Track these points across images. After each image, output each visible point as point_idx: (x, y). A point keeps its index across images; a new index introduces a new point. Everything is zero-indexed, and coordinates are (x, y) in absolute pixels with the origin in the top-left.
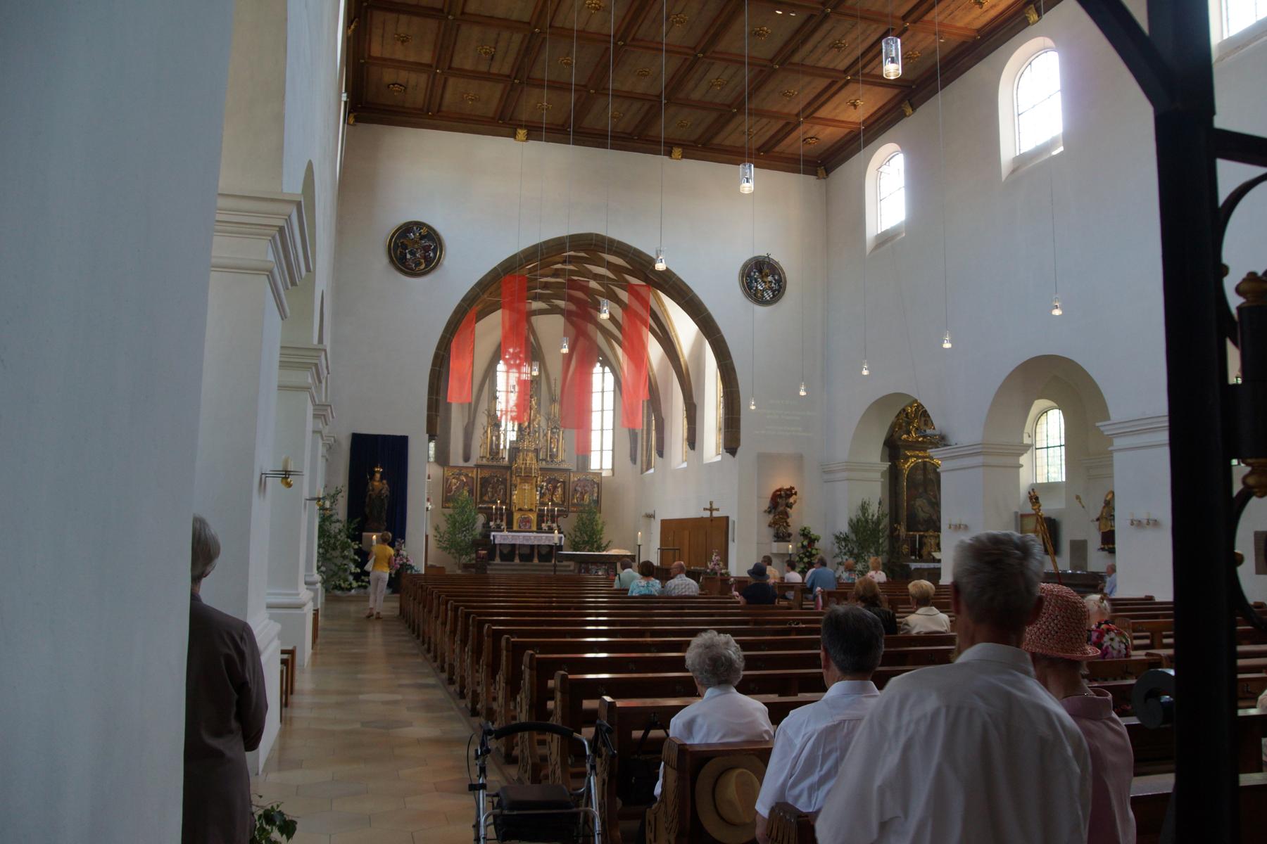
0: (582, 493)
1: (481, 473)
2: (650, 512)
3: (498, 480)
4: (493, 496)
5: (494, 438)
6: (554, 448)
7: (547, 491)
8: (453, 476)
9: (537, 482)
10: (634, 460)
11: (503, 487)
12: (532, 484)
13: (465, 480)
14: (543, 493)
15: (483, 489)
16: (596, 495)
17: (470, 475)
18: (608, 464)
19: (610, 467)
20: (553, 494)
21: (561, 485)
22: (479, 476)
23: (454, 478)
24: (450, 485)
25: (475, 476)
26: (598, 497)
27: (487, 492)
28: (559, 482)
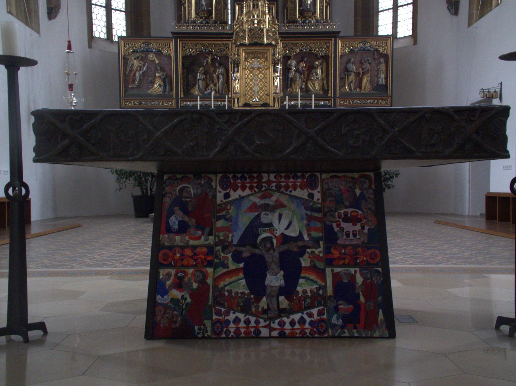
0: (357, 74)
1: (183, 47)
3: (213, 60)
4: (207, 86)
7: (298, 75)
8: (138, 55)
9: (274, 55)
11: (221, 70)
12: (266, 59)
13: (157, 62)
14: (292, 78)
15: (190, 76)
16: (382, 76)
19: (410, 33)
20: (308, 79)
21: (321, 64)
22: (180, 55)
23: (138, 58)
24: (131, 71)
25: (173, 54)
26: (386, 78)
28: (317, 59)
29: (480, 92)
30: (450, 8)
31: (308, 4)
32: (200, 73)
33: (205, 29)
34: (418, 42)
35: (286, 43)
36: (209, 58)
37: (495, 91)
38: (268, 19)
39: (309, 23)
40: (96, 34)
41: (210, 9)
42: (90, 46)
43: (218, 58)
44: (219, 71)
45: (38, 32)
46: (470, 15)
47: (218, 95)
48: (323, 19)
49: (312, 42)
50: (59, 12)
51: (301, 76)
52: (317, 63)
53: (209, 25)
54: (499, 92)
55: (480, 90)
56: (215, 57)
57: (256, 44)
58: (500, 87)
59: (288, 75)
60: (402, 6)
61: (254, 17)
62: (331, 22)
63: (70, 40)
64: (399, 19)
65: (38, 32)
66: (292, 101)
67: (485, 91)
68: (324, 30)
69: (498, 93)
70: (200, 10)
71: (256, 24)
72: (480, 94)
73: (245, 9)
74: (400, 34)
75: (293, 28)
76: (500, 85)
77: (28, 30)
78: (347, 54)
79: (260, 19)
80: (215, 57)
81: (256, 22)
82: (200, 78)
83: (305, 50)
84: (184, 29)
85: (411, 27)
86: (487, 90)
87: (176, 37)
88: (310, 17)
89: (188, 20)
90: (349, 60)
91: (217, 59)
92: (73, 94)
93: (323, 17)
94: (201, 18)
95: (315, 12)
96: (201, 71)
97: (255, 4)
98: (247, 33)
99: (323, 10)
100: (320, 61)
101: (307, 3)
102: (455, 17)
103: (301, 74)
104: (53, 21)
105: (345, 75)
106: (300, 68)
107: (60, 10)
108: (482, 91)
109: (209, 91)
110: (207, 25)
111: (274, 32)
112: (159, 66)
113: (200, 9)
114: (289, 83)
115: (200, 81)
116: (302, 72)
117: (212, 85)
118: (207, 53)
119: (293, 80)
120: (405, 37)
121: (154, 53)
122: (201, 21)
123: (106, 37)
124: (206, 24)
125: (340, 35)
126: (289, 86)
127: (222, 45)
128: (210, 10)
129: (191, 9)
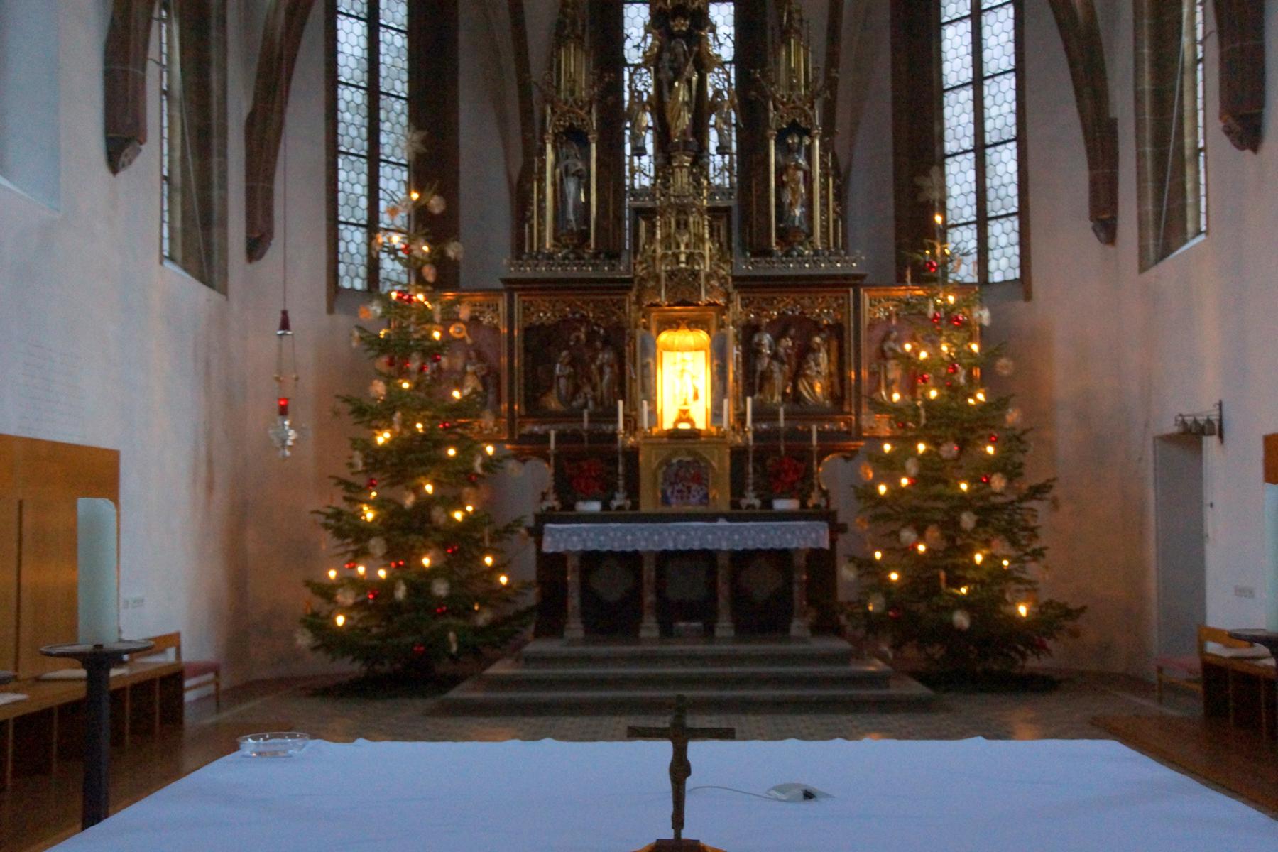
2: (1204, 408)
3: (592, 335)
4: (577, 389)
5: (571, 186)
6: (791, 204)
7: (776, 366)
10: (1106, 228)
11: (605, 356)
13: (469, 341)
14: (763, 373)
15: (540, 369)
17: (486, 320)
18: (1004, 266)
19: (1015, 274)
20: (797, 375)
21: (825, 340)
27: (551, 382)
29: (1176, 420)
30: (1097, 229)
31: (795, 216)
32: (561, 362)
33: (574, 271)
34: (1034, 295)
35: (748, 298)
36: (580, 330)
37: (1209, 421)
38: (710, 250)
39: (799, 255)
40: (345, 283)
41: (584, 228)
42: (331, 310)
43: (602, 331)
44: (603, 358)
45: (223, 290)
46: (1142, 249)
47: (600, 410)
48: (828, 248)
49: (807, 295)
50: (270, 244)
51: (783, 369)
52: (818, 340)
53: (582, 262)
54: (1216, 424)
55: (1176, 418)
56: (596, 328)
57: (683, 303)
58: (1217, 412)
59: (755, 366)
60: (997, 218)
61: (678, 247)
62: (846, 255)
63: (288, 308)
64: (991, 242)
65: (223, 290)
66: (764, 421)
67: (1187, 418)
68: (832, 272)
69: (1213, 424)
70: (564, 231)
71: (683, 262)
72: (1176, 425)
73: (658, 232)
74: (996, 277)
75: (762, 268)
76: (1218, 407)
77: (204, 289)
78: (883, 322)
79: (692, 251)
80: (596, 328)
81: (683, 258)
82: (561, 374)
83: (790, 313)
84: (528, 272)
85: (1016, 261)
86: (1192, 418)
87: (510, 288)
88: (801, 243)
89: (539, 252)
90: (891, 332)
91: (598, 332)
92: (287, 423)
93: (828, 244)
94: (566, 246)
95: (811, 233)
96: (565, 358)
97: (682, 222)
98: (663, 282)
99: (828, 228)
100: (824, 335)
101: (792, 214)
102: (1109, 249)
103: (782, 362)
104: (256, 264)
105: (879, 367)
106: (781, 350)
107: (273, 242)
108: (1180, 418)
109: (581, 401)
110: (577, 262)
111: (724, 277)
112: (475, 351)
113: (562, 228)
114: (757, 381)
115: (562, 382)
116: (785, 359)
117: (587, 389)
118: (578, 320)
119: (766, 377)
120: (1005, 282)
121: (465, 323)
122: (565, 254)
123: (366, 287)
124: (575, 259)
125: (865, 282)
126: (757, 389)
127: (610, 303)
128: (582, 231)
129: (545, 230)
